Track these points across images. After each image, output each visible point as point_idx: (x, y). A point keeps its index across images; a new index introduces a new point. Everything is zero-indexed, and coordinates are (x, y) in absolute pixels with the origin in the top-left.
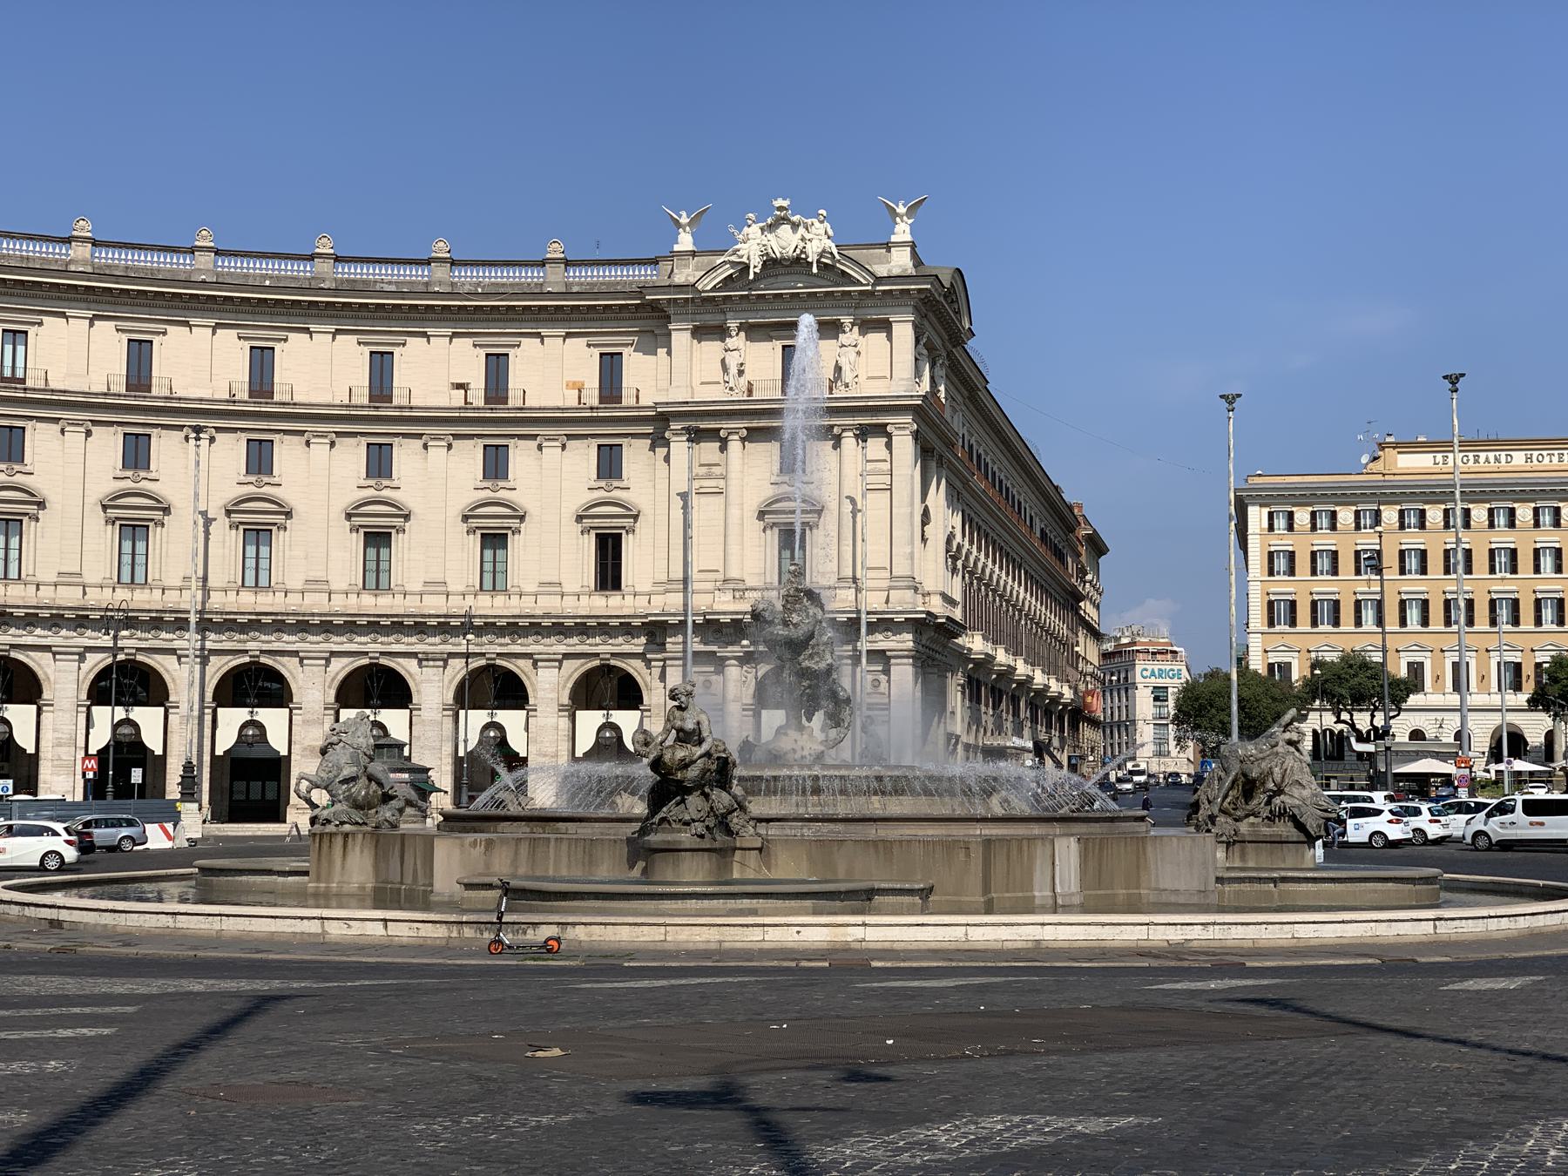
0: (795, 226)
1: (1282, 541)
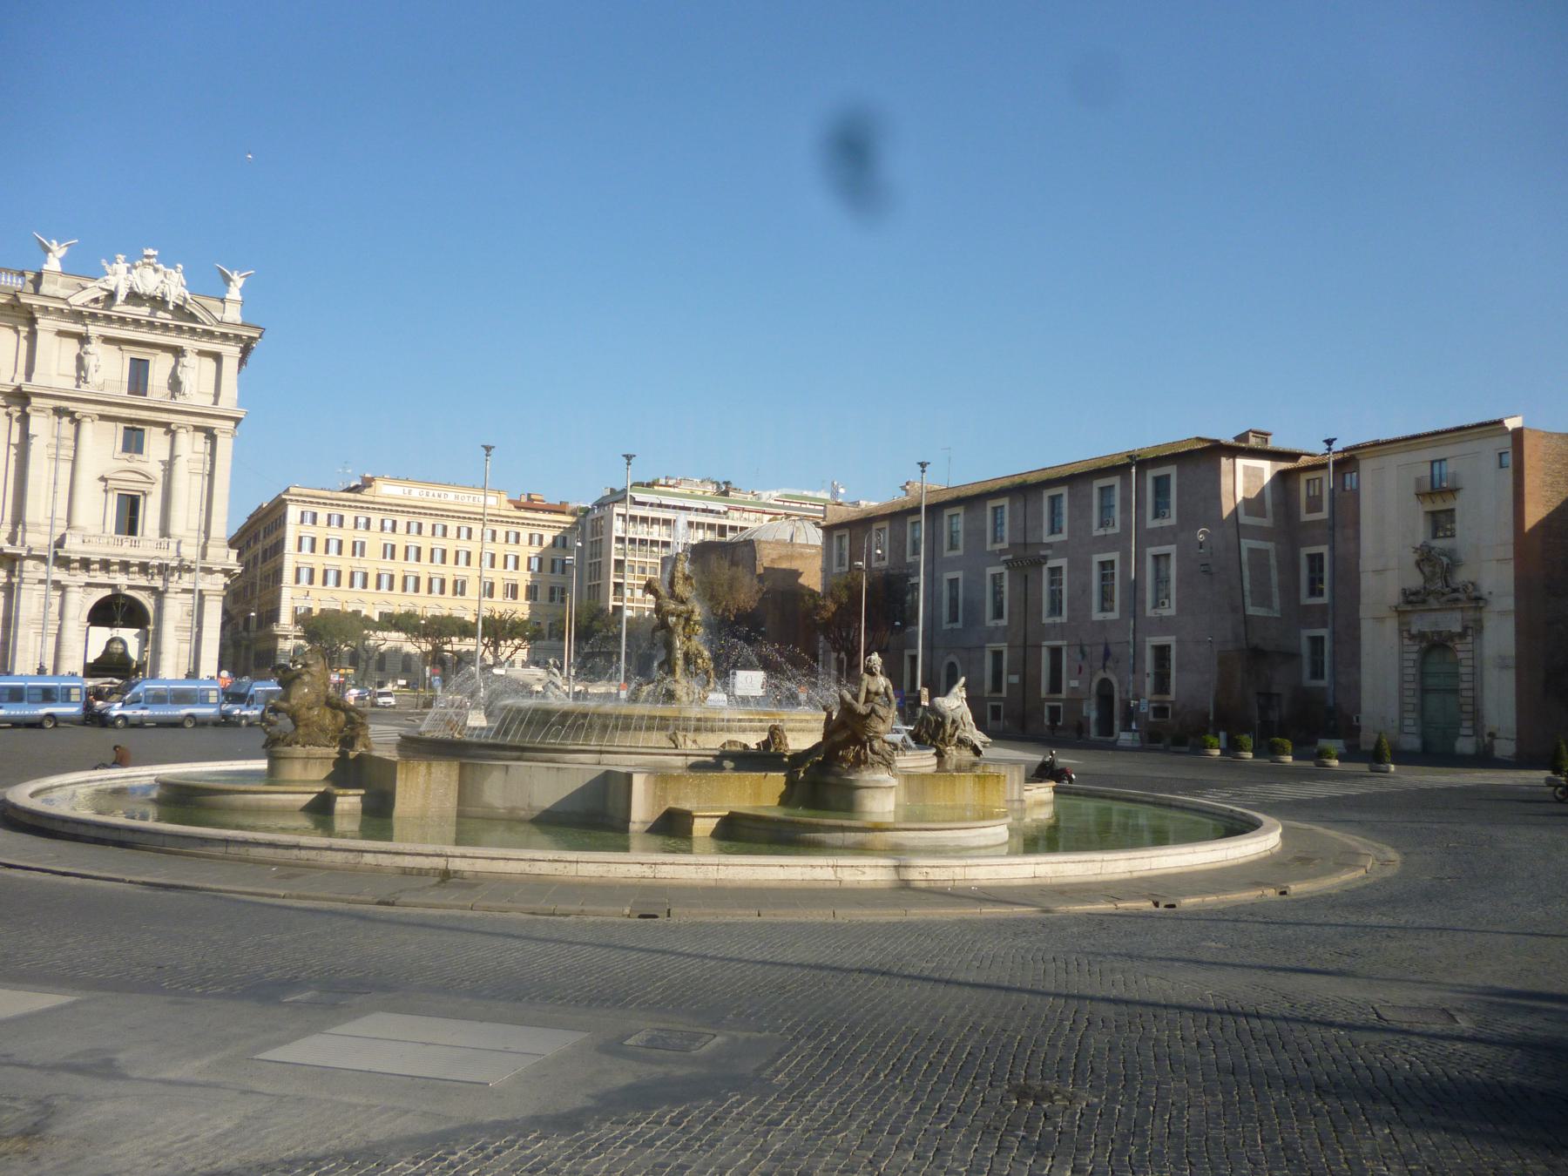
0: (156, 270)
1: (308, 531)
